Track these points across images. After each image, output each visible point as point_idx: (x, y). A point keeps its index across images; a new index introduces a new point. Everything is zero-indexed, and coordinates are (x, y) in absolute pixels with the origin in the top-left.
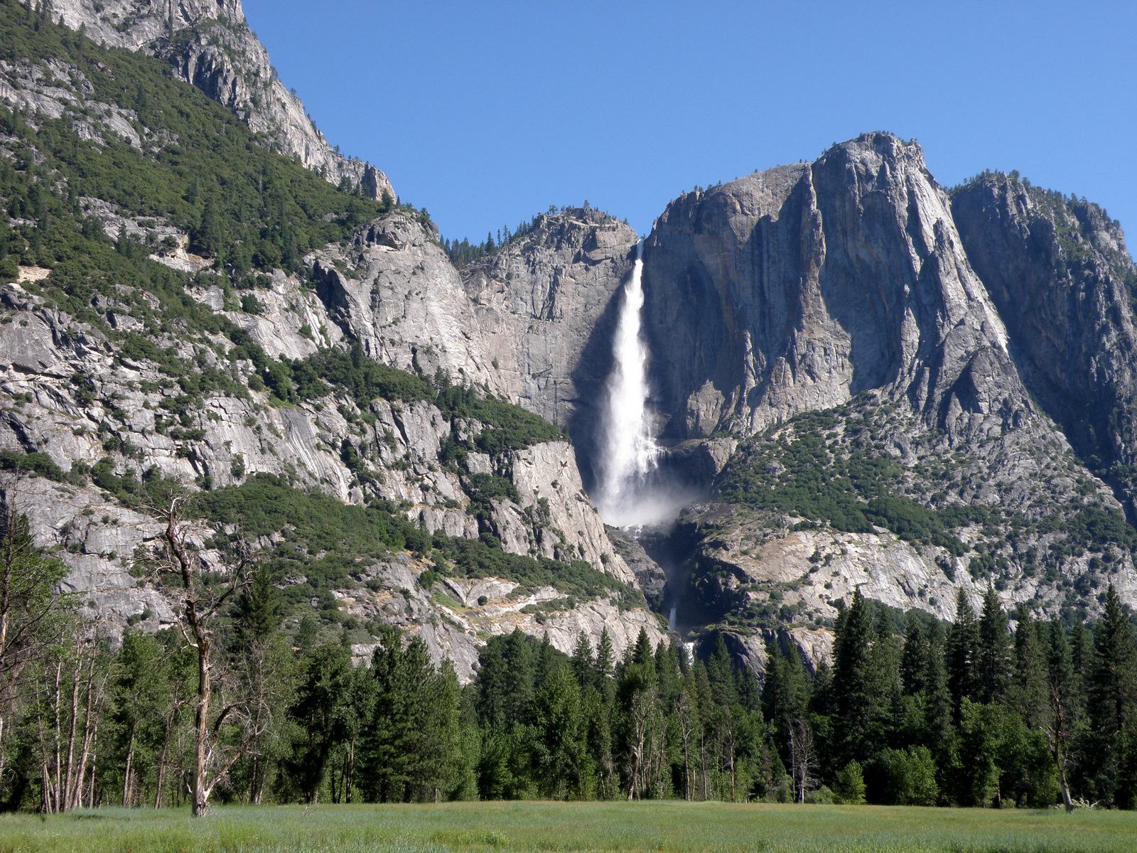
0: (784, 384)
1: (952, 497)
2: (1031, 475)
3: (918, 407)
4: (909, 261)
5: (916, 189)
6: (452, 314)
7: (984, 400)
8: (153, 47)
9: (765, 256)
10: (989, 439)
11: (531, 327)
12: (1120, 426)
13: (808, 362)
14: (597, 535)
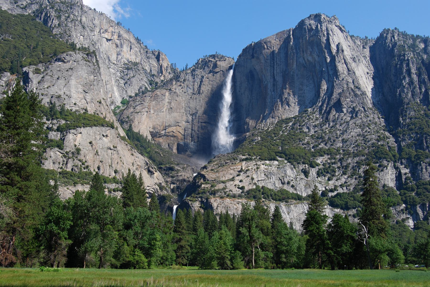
0: (278, 109)
1: (322, 145)
2: (358, 135)
3: (321, 113)
4: (326, 58)
5: (330, 32)
6: (81, 84)
7: (345, 108)
8: (34, 12)
9: (275, 64)
10: (344, 123)
11: (191, 98)
12: (402, 114)
13: (287, 100)
14: (116, 162)
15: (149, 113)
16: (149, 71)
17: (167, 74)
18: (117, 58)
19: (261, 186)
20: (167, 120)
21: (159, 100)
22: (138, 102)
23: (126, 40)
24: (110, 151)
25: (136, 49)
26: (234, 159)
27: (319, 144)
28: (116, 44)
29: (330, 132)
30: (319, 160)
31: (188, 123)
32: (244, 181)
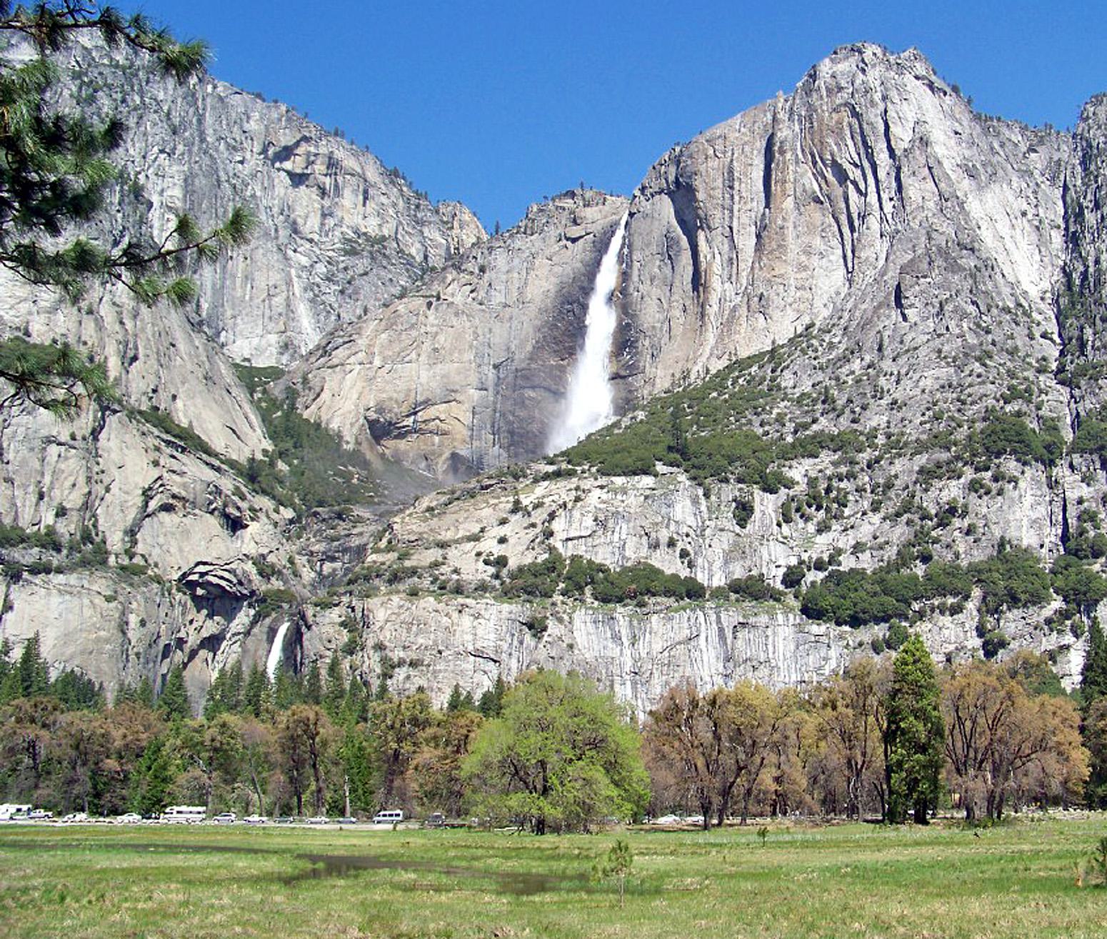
9: (737, 198)
14: (68, 483)
15: (368, 366)
16: (419, 258)
18: (323, 224)
23: (353, 175)
24: (54, 450)
25: (383, 199)
26: (516, 477)
27: (815, 421)
28: (319, 186)
29: (857, 382)
30: (798, 471)
32: (511, 541)
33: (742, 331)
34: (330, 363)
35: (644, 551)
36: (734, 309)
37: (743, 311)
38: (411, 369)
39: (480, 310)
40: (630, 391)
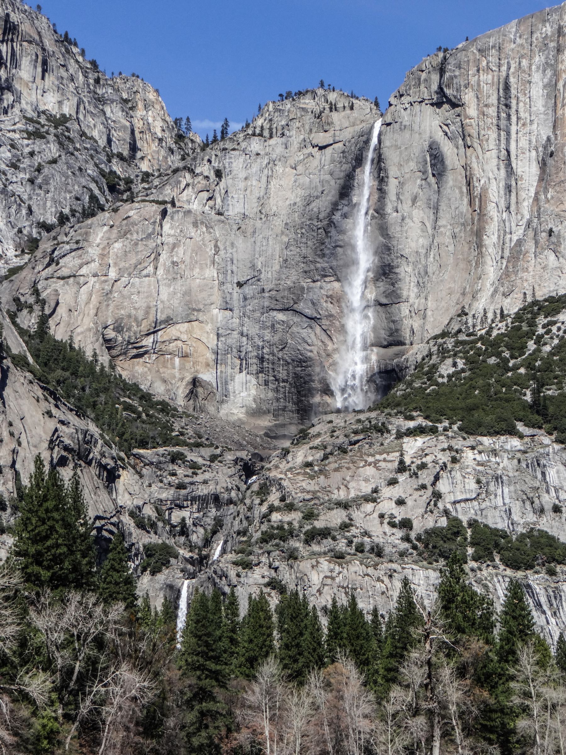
9: (514, 119)
15: (103, 278)
16: (102, 142)
17: (163, 152)
19: (464, 520)
20: (162, 302)
21: (135, 236)
22: (68, 243)
23: (30, 42)
31: (228, 313)
33: (530, 269)
34: (60, 273)
35: (531, 517)
36: (519, 243)
37: (530, 246)
38: (149, 285)
39: (219, 221)
40: (393, 322)
